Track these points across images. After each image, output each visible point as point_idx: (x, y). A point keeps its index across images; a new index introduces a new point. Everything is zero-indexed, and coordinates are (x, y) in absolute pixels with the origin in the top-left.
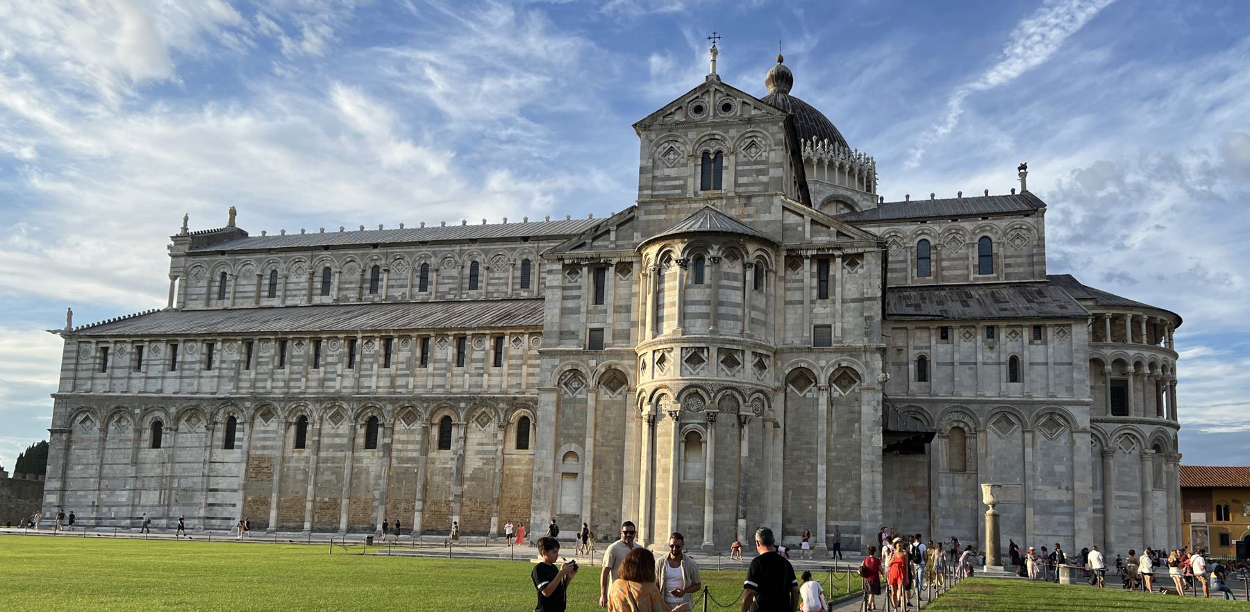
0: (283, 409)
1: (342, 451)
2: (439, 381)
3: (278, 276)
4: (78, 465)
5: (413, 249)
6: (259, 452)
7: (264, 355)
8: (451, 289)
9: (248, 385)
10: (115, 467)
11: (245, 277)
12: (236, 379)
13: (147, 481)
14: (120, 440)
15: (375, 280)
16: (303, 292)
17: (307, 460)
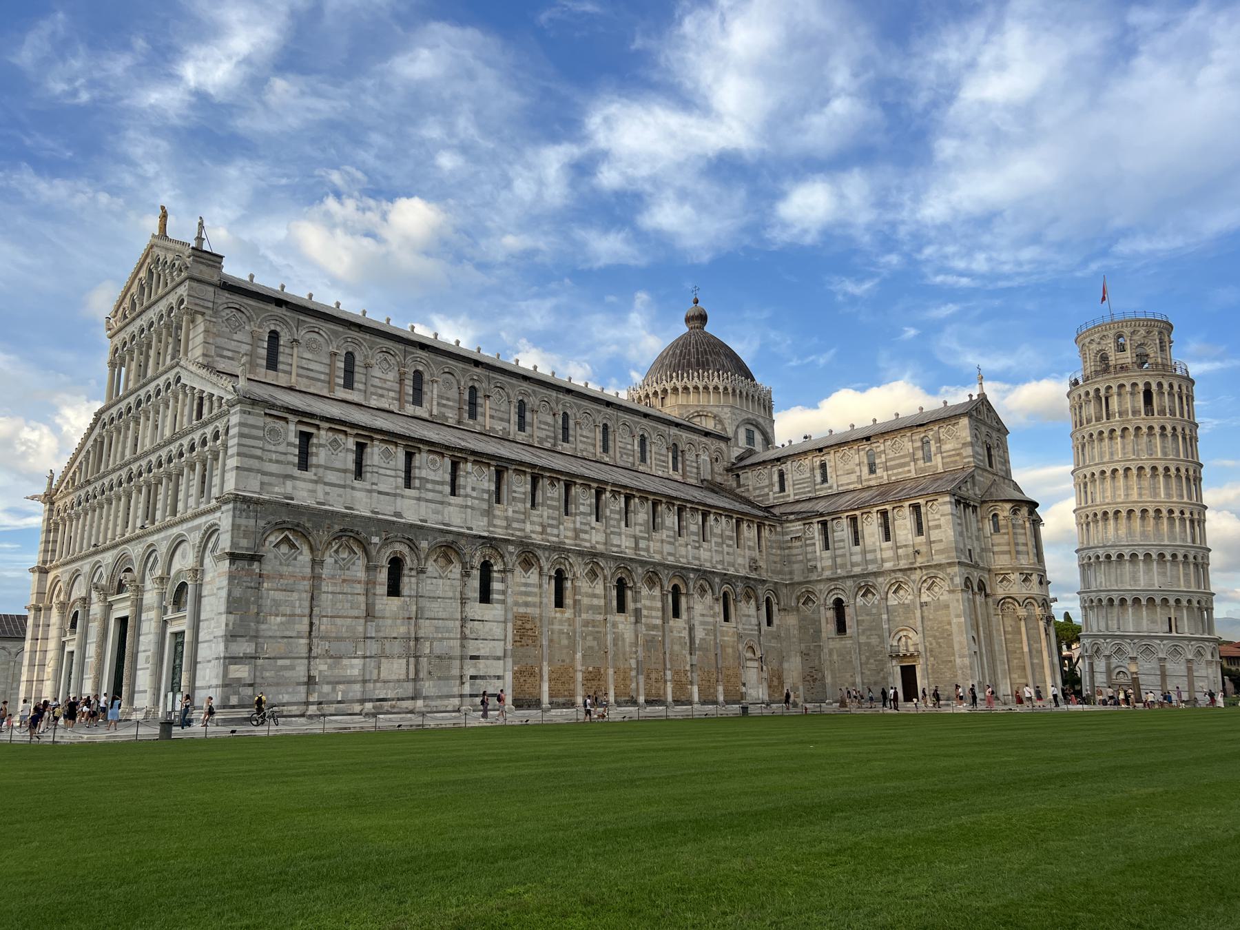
0: (547, 559)
1: (600, 614)
2: (667, 548)
3: (357, 363)
4: (277, 615)
5: (514, 381)
6: (522, 610)
7: (517, 489)
8: (548, 437)
9: (504, 524)
10: (338, 621)
11: (309, 348)
12: (489, 513)
13: (387, 644)
14: (344, 581)
15: (473, 404)
16: (392, 394)
17: (571, 622)
